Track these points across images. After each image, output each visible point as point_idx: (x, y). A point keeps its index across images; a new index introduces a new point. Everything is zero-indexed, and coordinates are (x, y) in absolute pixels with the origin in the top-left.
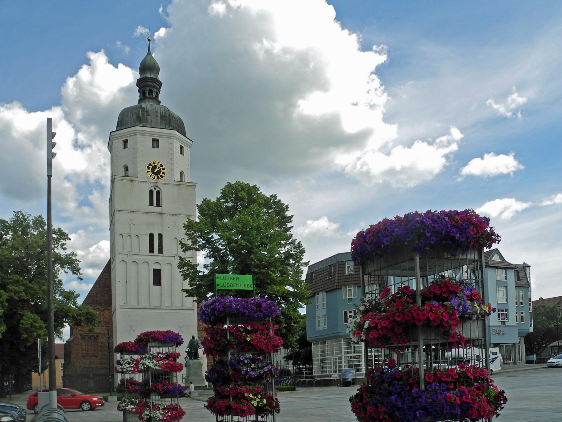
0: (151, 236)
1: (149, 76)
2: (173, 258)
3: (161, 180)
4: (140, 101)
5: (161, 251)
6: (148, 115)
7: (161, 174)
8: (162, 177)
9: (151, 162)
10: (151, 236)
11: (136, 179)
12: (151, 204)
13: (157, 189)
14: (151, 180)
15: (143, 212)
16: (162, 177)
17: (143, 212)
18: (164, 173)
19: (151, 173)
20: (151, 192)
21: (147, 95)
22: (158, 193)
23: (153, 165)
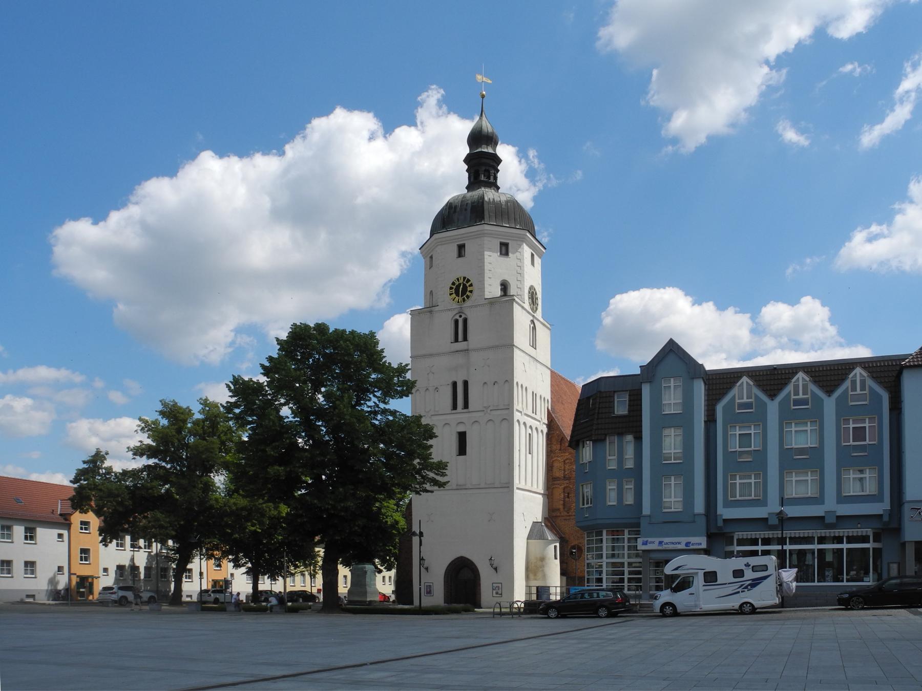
0: (455, 385)
1: (485, 150)
2: (481, 414)
3: (468, 303)
4: (469, 188)
5: (466, 406)
6: (455, 212)
7: (468, 293)
8: (468, 297)
9: (453, 279)
10: (455, 385)
11: (436, 309)
12: (456, 340)
13: (463, 316)
14: (455, 305)
15: (444, 354)
16: (468, 297)
17: (444, 354)
18: (471, 292)
19: (454, 295)
20: (456, 322)
21: (483, 178)
22: (465, 321)
23: (457, 283)
